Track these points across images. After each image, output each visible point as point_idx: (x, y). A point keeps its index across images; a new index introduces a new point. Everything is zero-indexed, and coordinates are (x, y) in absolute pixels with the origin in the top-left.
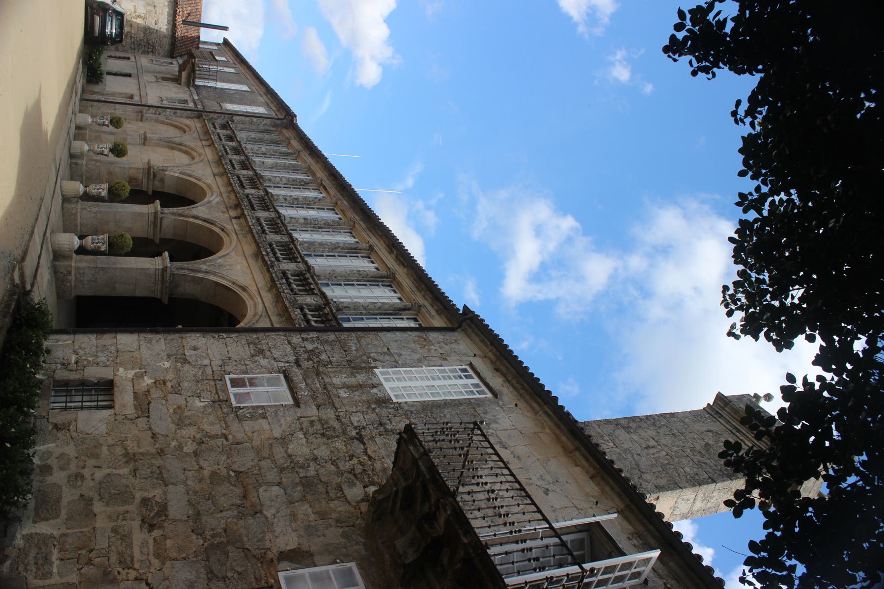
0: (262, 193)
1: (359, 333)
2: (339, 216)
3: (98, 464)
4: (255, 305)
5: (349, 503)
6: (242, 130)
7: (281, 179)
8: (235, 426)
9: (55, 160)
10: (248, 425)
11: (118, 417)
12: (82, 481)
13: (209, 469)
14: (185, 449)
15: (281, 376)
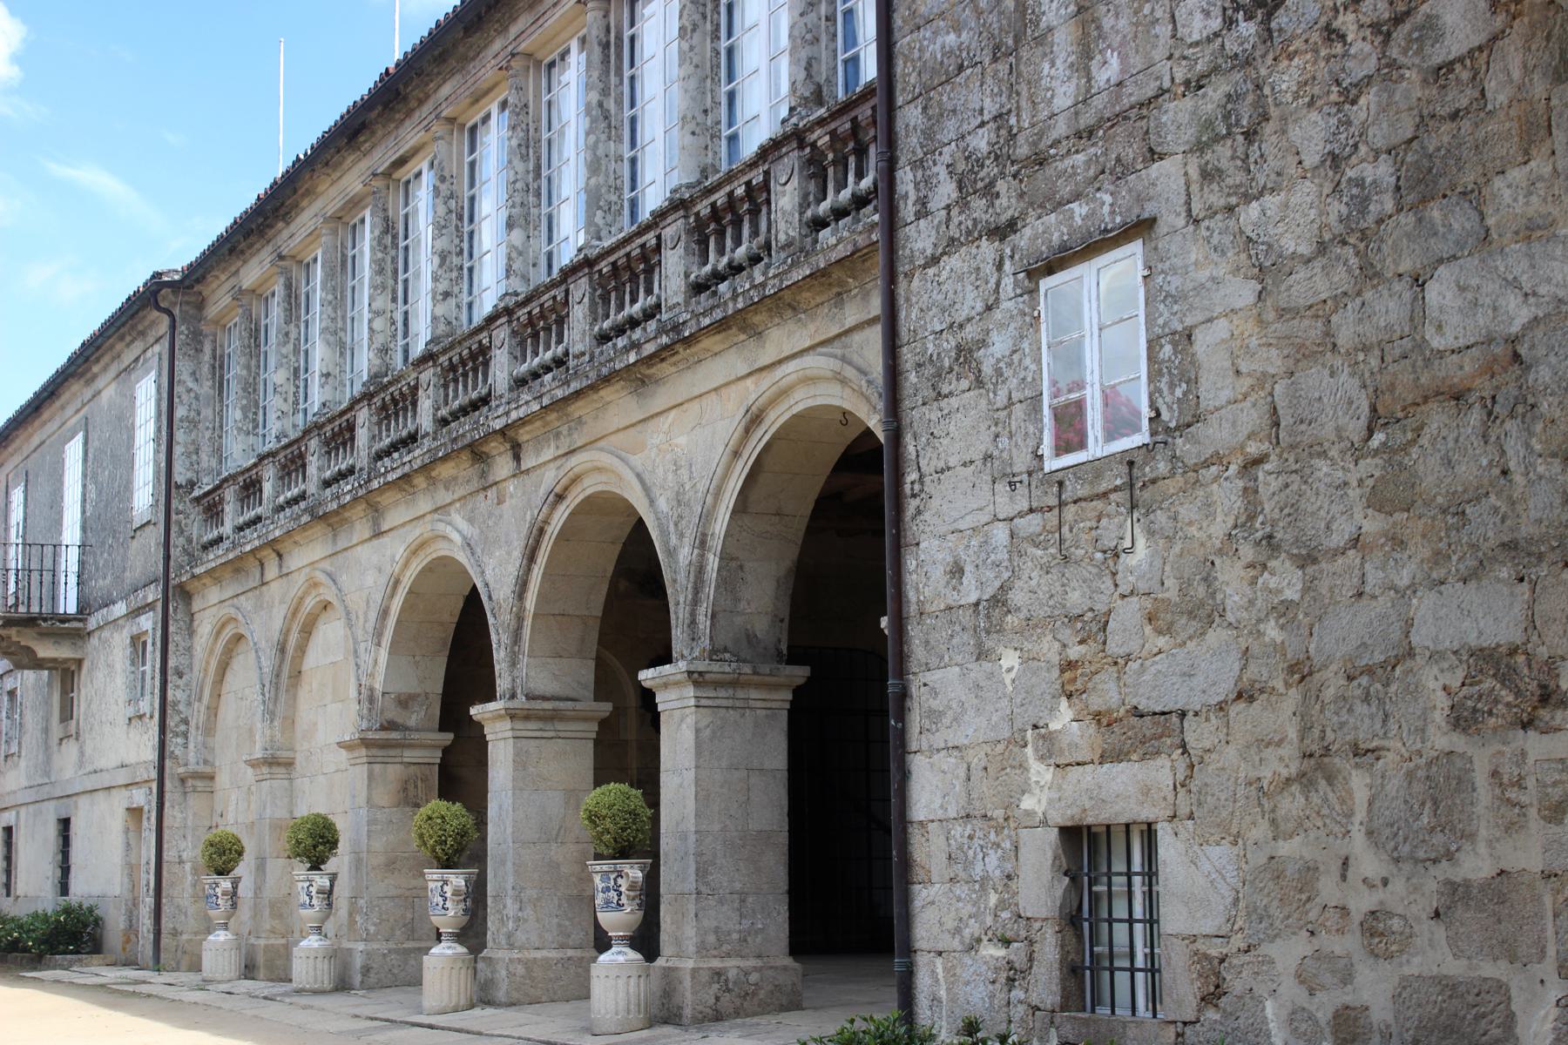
0: (428, 375)
1: (898, 21)
2: (494, 109)
3: (1335, 867)
4: (809, 380)
5: (1494, 38)
6: (218, 452)
7: (378, 313)
8: (1215, 434)
9: (358, 1034)
10: (1215, 389)
11: (1184, 810)
12: (1390, 915)
13: (1358, 516)
14: (1291, 594)
15: (1046, 283)
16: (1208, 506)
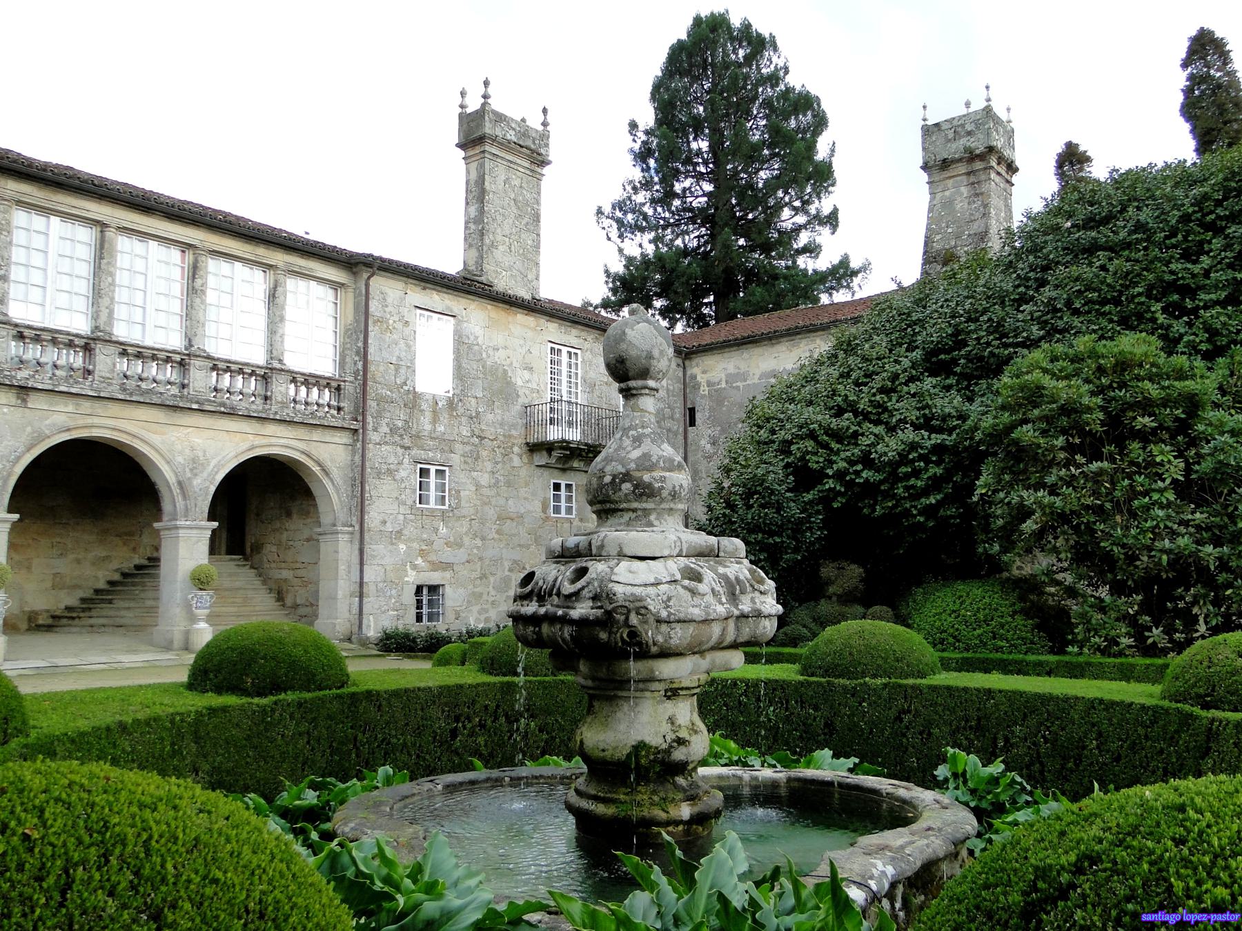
16: (462, 526)
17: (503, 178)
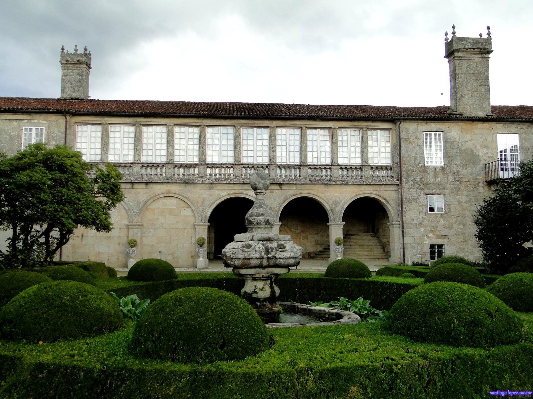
17: (466, 65)
